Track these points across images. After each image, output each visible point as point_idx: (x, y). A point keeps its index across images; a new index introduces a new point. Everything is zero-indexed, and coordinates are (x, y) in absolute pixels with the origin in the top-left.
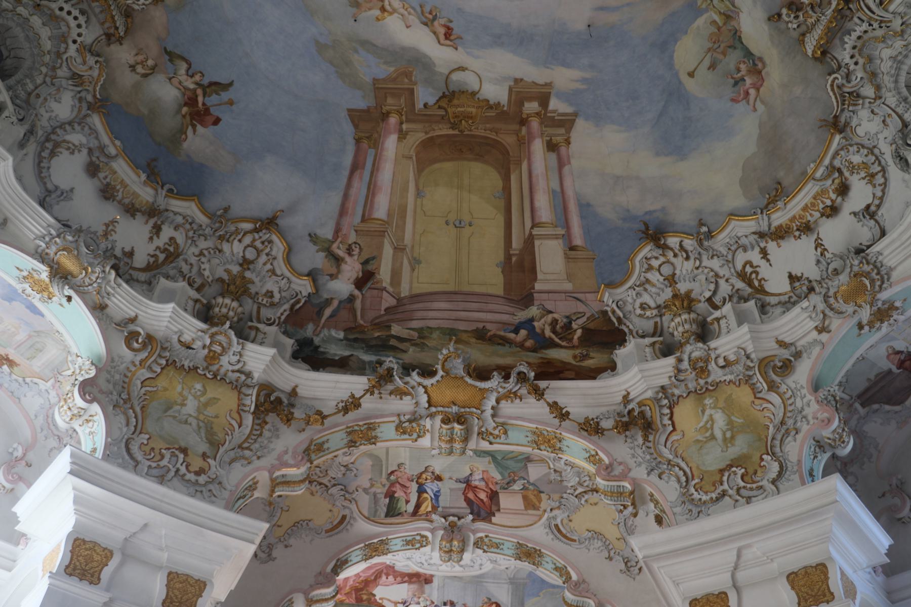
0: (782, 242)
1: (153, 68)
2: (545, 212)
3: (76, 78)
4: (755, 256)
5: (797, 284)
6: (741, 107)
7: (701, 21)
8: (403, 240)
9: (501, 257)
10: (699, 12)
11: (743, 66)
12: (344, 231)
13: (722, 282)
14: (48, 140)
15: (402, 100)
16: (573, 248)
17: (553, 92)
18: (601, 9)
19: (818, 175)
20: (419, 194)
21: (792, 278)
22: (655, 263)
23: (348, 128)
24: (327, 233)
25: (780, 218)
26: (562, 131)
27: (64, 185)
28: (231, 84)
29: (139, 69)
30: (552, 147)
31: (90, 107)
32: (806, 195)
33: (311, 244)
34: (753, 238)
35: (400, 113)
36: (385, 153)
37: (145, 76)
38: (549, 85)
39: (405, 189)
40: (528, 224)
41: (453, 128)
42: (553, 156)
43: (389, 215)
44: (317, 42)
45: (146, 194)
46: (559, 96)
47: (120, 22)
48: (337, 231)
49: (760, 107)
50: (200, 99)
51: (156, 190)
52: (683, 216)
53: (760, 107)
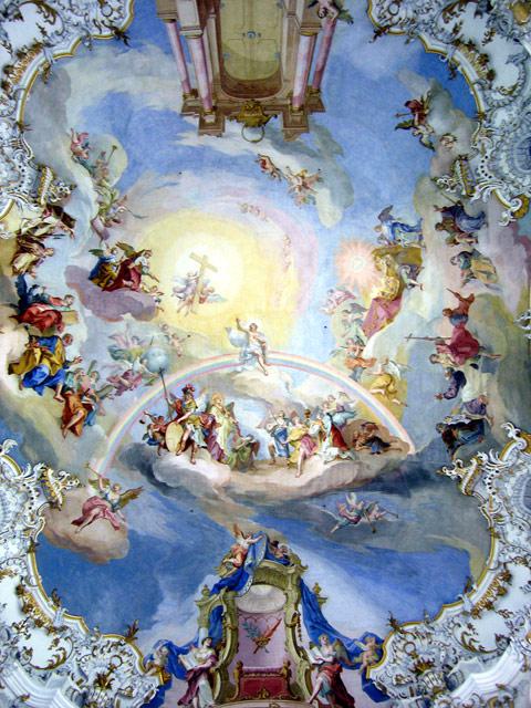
0: (34, 42)
1: (442, 139)
2: (194, 45)
3: (489, 135)
4: (50, 29)
5: (16, 13)
6: (81, 131)
7: (116, 181)
8: (289, 21)
9: (221, 11)
10: (115, 186)
11: (85, 156)
12: (329, 26)
13: (67, 6)
14: (515, 97)
15: (290, 118)
16: (173, 21)
17: (197, 130)
18: (175, 184)
19: (23, 93)
20: (279, 55)
21: (19, 17)
22: (115, 14)
23: (325, 99)
24: (341, 24)
25: (39, 59)
26: (190, 104)
27: (512, 65)
28: (397, 128)
29: (451, 138)
30: (195, 93)
31: (484, 116)
32: (25, 81)
33: (353, 15)
34: (53, 42)
35: (292, 111)
36: (301, 83)
37: (447, 134)
38: (201, 134)
39: (288, 58)
40: (205, 37)
41: (259, 102)
42: (193, 87)
43: (298, 40)
44: (342, 154)
45: (460, 56)
46: (193, 127)
47: (458, 168)
48: (333, 26)
49: (69, 131)
50: (416, 119)
51: (452, 59)
52: (103, 51)
53: (69, 131)
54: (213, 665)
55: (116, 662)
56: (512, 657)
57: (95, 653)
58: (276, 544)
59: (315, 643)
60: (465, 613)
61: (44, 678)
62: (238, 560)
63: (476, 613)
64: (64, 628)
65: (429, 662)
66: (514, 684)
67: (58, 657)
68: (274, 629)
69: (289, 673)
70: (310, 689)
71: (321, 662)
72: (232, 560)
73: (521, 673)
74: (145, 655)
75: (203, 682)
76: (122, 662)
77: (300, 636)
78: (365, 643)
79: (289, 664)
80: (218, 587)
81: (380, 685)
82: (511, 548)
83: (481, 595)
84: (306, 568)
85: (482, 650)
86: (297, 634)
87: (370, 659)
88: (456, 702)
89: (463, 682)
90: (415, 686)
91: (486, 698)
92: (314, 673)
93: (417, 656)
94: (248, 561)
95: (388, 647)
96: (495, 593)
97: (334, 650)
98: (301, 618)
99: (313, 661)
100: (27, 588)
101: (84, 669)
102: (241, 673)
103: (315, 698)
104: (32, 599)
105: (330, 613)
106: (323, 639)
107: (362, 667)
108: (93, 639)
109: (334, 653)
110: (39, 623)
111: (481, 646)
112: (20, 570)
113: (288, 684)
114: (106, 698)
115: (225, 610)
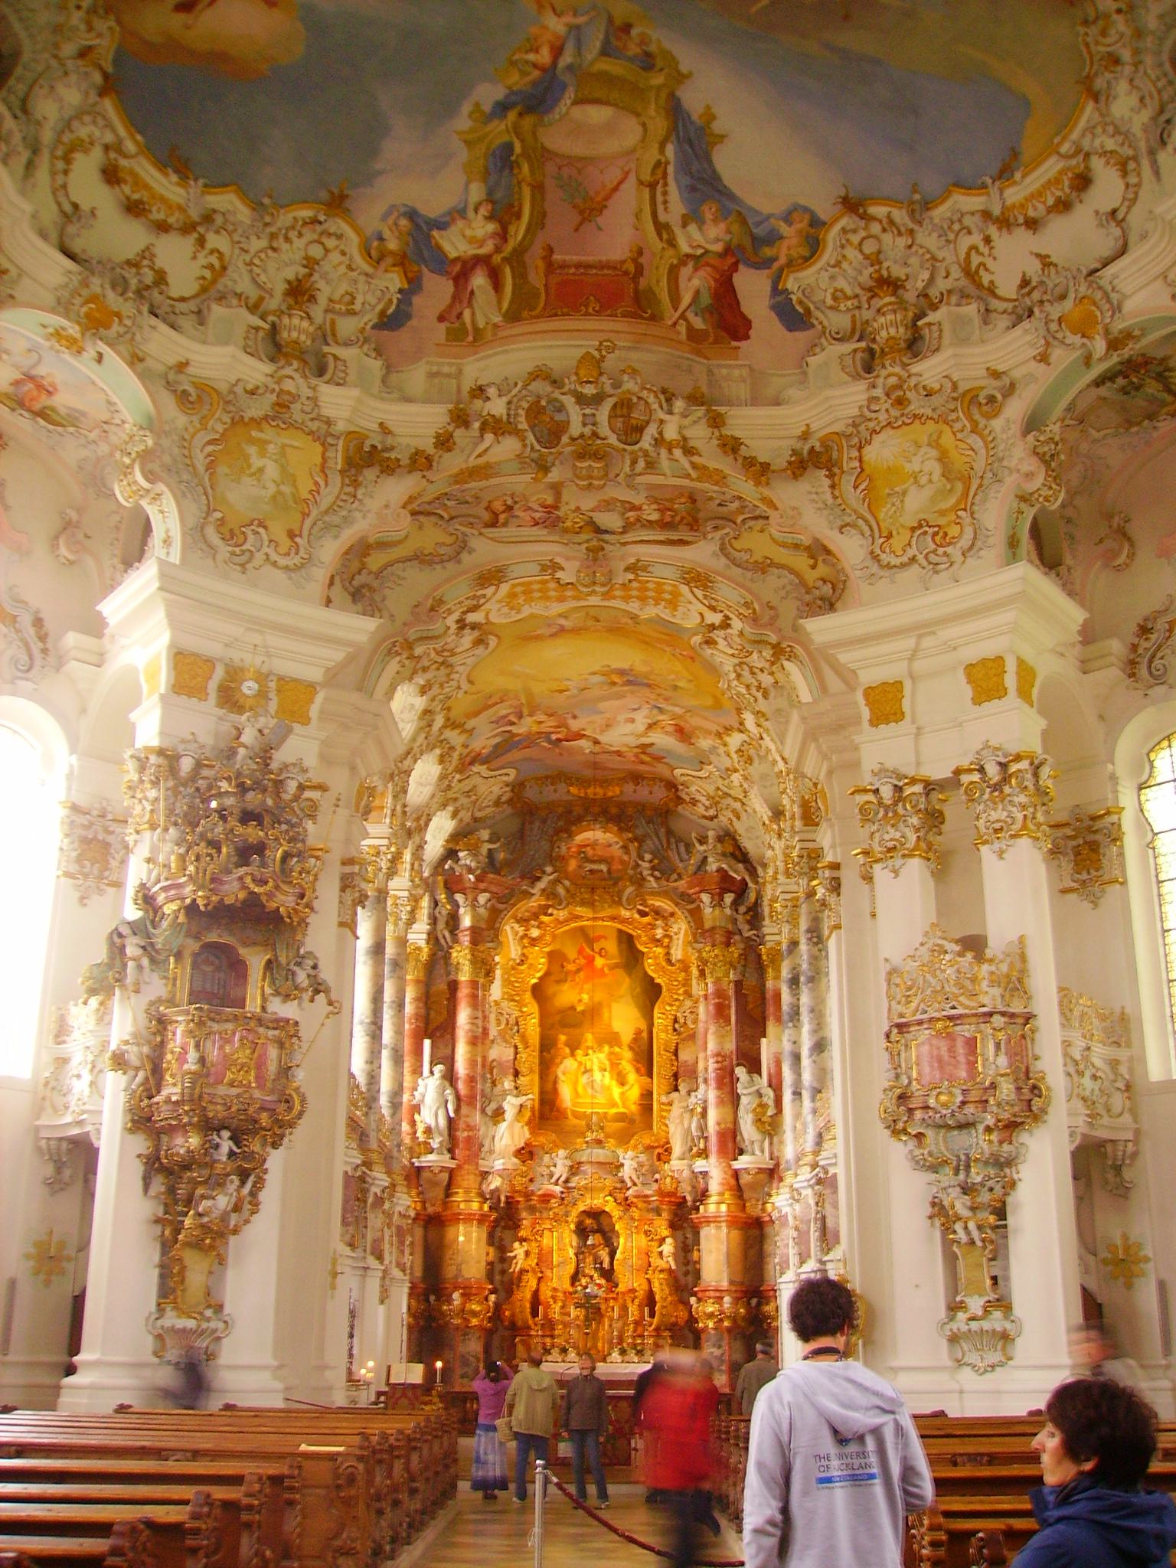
54: (498, 249)
55: (316, 251)
56: (1028, 338)
57: (275, 245)
58: (627, 28)
59: (692, 217)
60: (986, 215)
61: (200, 316)
62: (544, 57)
63: (1005, 223)
64: (208, 218)
65: (898, 279)
66: (1016, 374)
67: (211, 267)
68: (616, 189)
69: (640, 271)
70: (675, 300)
71: (699, 252)
72: (531, 57)
73: (1033, 363)
74: (369, 232)
75: (479, 280)
76: (327, 251)
77: (665, 202)
78: (790, 223)
79: (640, 252)
80: (502, 108)
81: (800, 302)
82: (1110, 129)
83: (1027, 193)
84: (689, 76)
85: (992, 291)
86: (659, 198)
87: (794, 253)
88: (913, 381)
89: (937, 350)
90: (867, 315)
91: (963, 387)
92: (686, 271)
93: (880, 263)
94: (567, 59)
95: (832, 236)
96: (1051, 201)
97: (729, 232)
98: (671, 169)
99: (685, 248)
100: (123, 162)
101: (263, 278)
102: (550, 267)
103: (683, 316)
104: (139, 183)
105: (727, 163)
106: (708, 211)
107: (776, 266)
108: (268, 219)
109: (727, 238)
110: (163, 227)
111: (992, 282)
112: (97, 133)
113: (636, 291)
114: (311, 329)
115: (518, 149)
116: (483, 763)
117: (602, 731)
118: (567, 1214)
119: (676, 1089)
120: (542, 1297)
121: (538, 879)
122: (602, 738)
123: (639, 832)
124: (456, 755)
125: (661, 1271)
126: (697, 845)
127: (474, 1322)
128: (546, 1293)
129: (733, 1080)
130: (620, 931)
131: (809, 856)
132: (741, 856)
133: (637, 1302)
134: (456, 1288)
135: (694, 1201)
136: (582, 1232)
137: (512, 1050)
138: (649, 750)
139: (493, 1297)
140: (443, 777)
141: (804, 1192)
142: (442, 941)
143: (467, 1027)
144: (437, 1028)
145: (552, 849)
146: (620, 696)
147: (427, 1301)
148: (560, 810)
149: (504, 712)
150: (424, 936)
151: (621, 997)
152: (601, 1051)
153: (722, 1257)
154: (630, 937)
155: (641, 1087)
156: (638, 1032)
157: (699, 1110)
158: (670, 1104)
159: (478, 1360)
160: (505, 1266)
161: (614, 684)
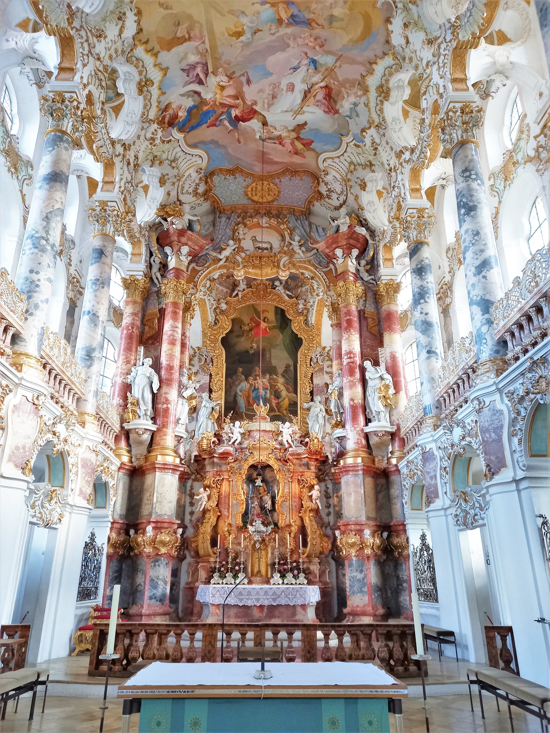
116: (181, 130)
117: (269, 105)
118: (240, 468)
119: (312, 400)
120: (220, 531)
121: (225, 249)
122: (270, 119)
123: (290, 225)
124: (155, 91)
125: (311, 511)
126: (332, 222)
127: (163, 550)
128: (223, 527)
129: (363, 370)
130: (276, 308)
131: (462, 112)
132: (363, 223)
133: (292, 535)
134: (149, 523)
135: (333, 461)
136: (250, 480)
137: (208, 378)
138: (304, 134)
139: (180, 531)
140: (145, 120)
141: (487, 400)
142: (156, 281)
143: (169, 333)
144: (149, 338)
145: (234, 234)
146: (284, 47)
147: (127, 533)
148: (239, 211)
149: (193, 58)
150: (142, 273)
151: (278, 345)
152: (264, 378)
153: (361, 498)
154: (283, 311)
155: (289, 400)
156: (288, 366)
157: (337, 393)
158: (309, 409)
159: (166, 583)
160: (194, 508)
161: (280, 21)
